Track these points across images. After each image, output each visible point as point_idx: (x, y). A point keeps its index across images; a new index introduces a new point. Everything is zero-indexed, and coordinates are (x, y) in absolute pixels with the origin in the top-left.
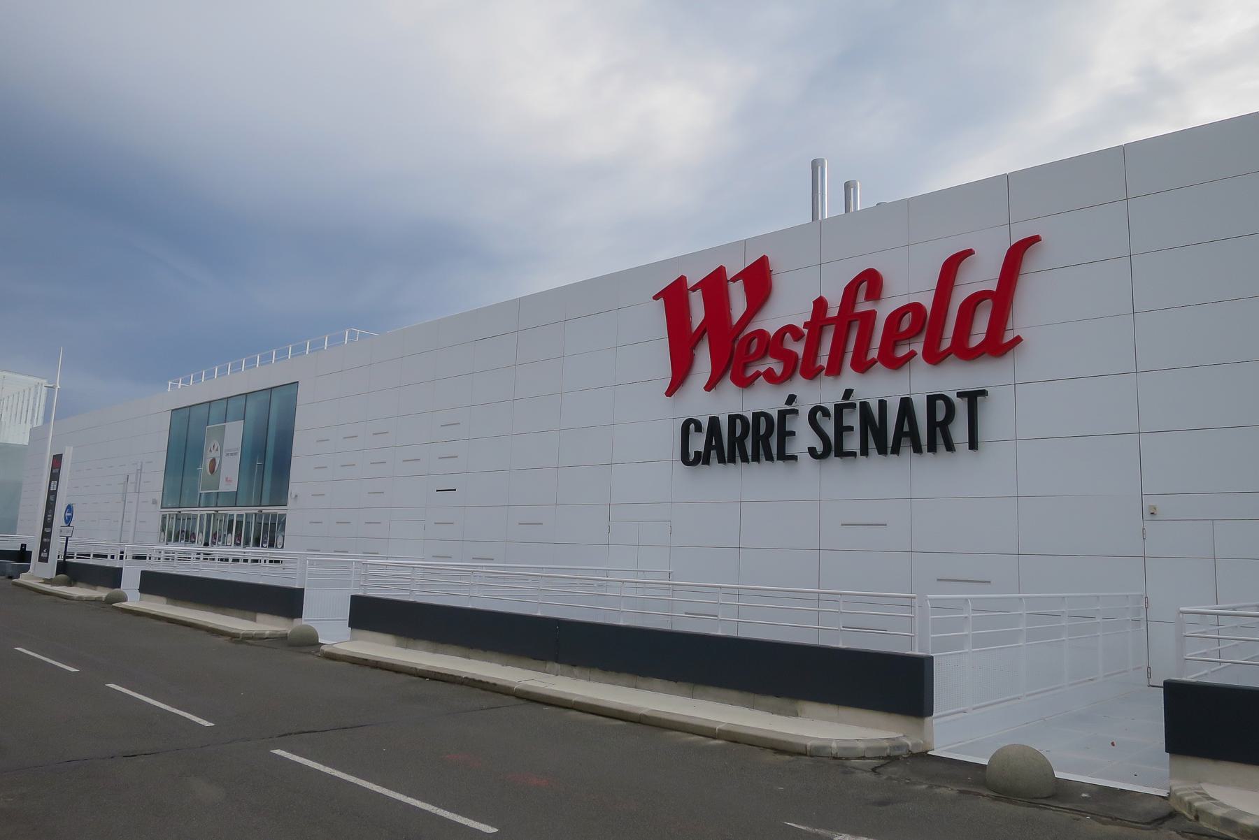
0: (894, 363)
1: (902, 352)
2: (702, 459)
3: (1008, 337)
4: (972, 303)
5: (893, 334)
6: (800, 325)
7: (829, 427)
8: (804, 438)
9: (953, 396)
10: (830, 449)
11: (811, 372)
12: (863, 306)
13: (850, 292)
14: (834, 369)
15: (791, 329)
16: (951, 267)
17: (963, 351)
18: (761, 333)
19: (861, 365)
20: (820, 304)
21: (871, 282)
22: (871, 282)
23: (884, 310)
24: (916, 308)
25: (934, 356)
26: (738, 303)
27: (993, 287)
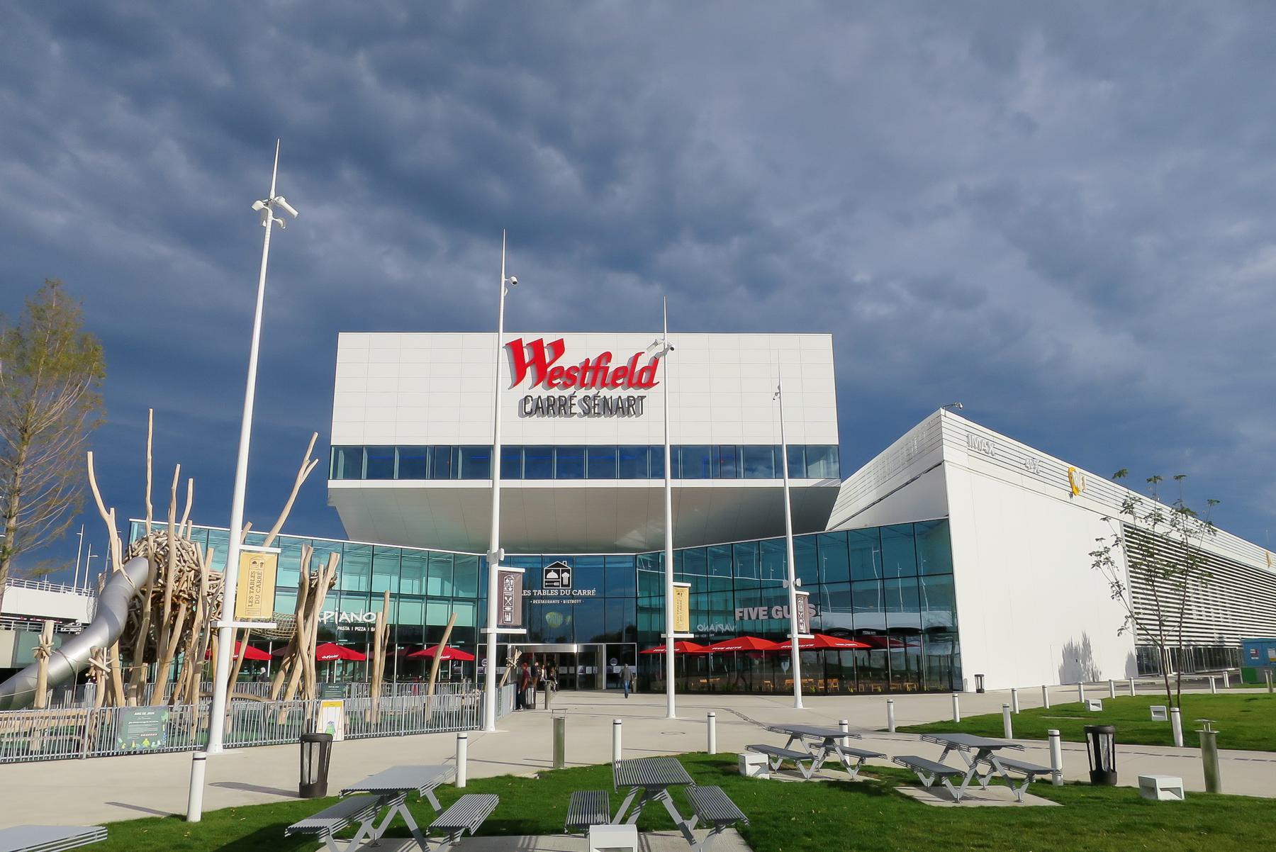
0: (615, 385)
2: (530, 414)
3: (654, 382)
4: (643, 370)
6: (578, 366)
8: (576, 409)
9: (636, 397)
10: (587, 413)
11: (583, 385)
12: (602, 365)
13: (600, 358)
14: (593, 384)
15: (575, 368)
16: (638, 355)
17: (640, 385)
18: (561, 368)
19: (604, 385)
20: (588, 361)
21: (607, 356)
22: (607, 356)
23: (612, 366)
25: (630, 385)
27: (651, 365)
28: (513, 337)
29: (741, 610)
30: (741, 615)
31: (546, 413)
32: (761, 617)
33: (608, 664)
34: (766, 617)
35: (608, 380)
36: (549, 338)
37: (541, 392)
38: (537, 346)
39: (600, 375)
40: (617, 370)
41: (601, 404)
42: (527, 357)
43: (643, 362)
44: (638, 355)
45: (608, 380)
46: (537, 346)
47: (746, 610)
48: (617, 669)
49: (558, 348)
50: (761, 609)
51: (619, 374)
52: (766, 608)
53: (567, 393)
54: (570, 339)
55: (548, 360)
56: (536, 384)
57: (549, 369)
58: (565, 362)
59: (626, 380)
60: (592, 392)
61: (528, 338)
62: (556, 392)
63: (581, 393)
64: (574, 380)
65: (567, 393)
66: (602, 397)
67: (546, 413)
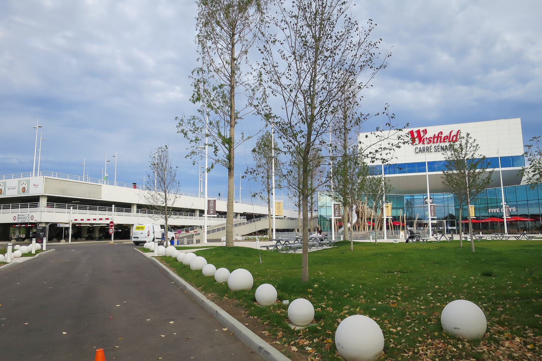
0: (444, 142)
1: (445, 141)
5: (444, 139)
6: (432, 137)
7: (437, 148)
8: (433, 150)
11: (434, 142)
13: (439, 134)
15: (431, 138)
16: (451, 132)
19: (440, 142)
20: (435, 135)
21: (441, 133)
22: (441, 133)
23: (443, 136)
24: (447, 136)
26: (422, 134)
27: (456, 134)
28: (410, 130)
29: (491, 209)
30: (491, 211)
31: (422, 152)
32: (497, 212)
33: (447, 226)
34: (499, 212)
35: (442, 140)
36: (421, 129)
37: (421, 146)
38: (418, 132)
39: (439, 139)
40: (445, 137)
41: (440, 148)
42: (416, 135)
43: (454, 133)
44: (451, 132)
45: (442, 140)
46: (418, 132)
47: (492, 210)
48: (450, 228)
49: (425, 132)
50: (497, 209)
51: (446, 138)
52: (499, 209)
53: (429, 145)
54: (428, 129)
55: (422, 136)
56: (419, 143)
57: (422, 139)
58: (427, 136)
59: (448, 141)
60: (437, 145)
61: (415, 129)
62: (426, 145)
63: (433, 145)
64: (430, 141)
65: (429, 145)
66: (440, 146)
67: (422, 152)
